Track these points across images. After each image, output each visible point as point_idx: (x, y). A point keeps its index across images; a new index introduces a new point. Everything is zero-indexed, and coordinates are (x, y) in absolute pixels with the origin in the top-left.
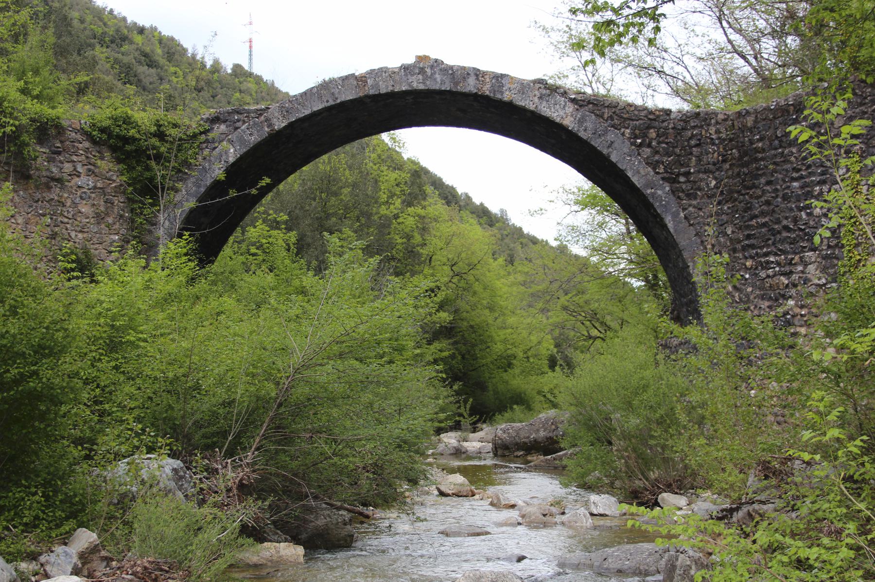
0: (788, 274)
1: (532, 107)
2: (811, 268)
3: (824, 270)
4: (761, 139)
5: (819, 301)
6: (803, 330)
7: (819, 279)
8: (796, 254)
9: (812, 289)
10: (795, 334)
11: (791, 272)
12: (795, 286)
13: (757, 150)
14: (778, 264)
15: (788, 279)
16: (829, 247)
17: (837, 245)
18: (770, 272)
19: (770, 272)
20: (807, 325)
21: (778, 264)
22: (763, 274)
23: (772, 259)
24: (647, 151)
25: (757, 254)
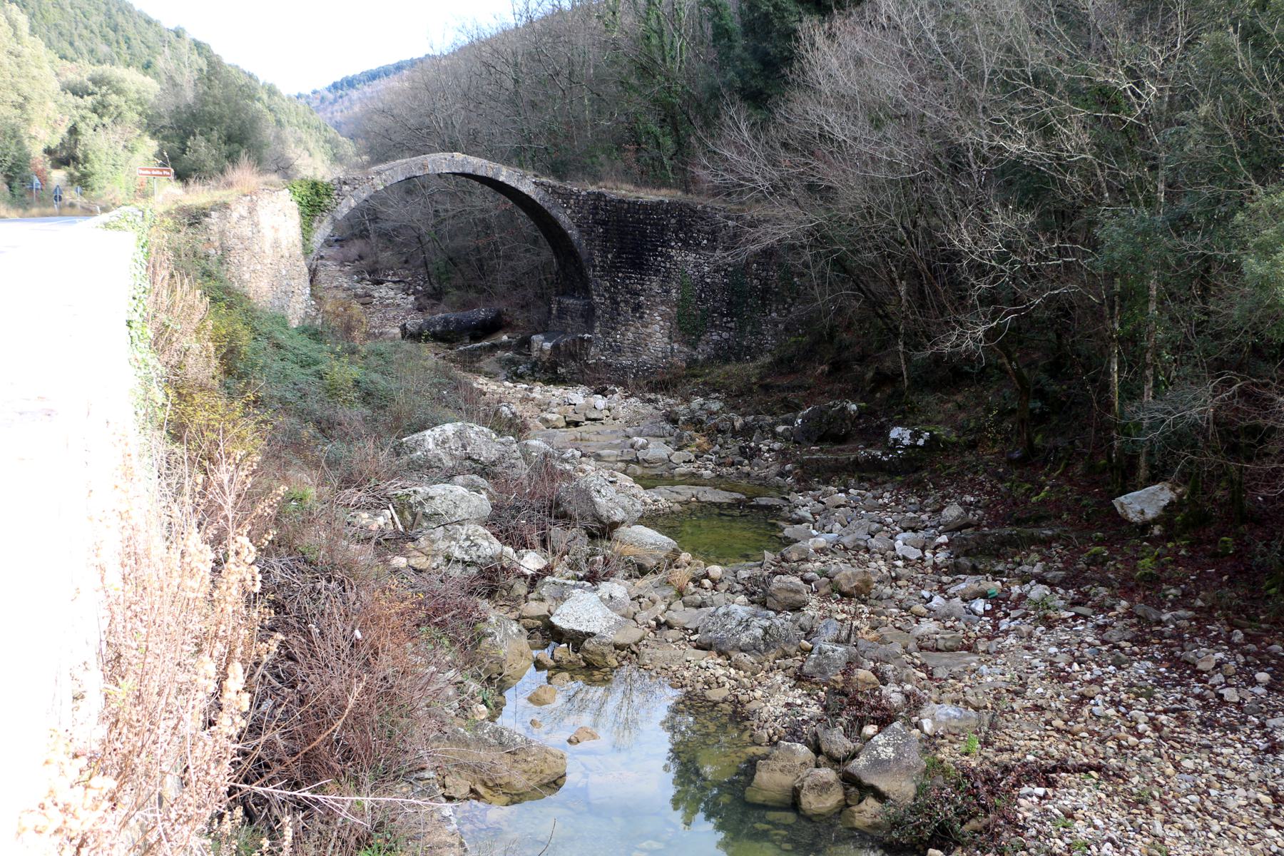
0: (642, 285)
1: (513, 185)
3: (661, 286)
5: (658, 300)
10: (643, 313)
20: (650, 309)
22: (628, 282)
24: (569, 211)
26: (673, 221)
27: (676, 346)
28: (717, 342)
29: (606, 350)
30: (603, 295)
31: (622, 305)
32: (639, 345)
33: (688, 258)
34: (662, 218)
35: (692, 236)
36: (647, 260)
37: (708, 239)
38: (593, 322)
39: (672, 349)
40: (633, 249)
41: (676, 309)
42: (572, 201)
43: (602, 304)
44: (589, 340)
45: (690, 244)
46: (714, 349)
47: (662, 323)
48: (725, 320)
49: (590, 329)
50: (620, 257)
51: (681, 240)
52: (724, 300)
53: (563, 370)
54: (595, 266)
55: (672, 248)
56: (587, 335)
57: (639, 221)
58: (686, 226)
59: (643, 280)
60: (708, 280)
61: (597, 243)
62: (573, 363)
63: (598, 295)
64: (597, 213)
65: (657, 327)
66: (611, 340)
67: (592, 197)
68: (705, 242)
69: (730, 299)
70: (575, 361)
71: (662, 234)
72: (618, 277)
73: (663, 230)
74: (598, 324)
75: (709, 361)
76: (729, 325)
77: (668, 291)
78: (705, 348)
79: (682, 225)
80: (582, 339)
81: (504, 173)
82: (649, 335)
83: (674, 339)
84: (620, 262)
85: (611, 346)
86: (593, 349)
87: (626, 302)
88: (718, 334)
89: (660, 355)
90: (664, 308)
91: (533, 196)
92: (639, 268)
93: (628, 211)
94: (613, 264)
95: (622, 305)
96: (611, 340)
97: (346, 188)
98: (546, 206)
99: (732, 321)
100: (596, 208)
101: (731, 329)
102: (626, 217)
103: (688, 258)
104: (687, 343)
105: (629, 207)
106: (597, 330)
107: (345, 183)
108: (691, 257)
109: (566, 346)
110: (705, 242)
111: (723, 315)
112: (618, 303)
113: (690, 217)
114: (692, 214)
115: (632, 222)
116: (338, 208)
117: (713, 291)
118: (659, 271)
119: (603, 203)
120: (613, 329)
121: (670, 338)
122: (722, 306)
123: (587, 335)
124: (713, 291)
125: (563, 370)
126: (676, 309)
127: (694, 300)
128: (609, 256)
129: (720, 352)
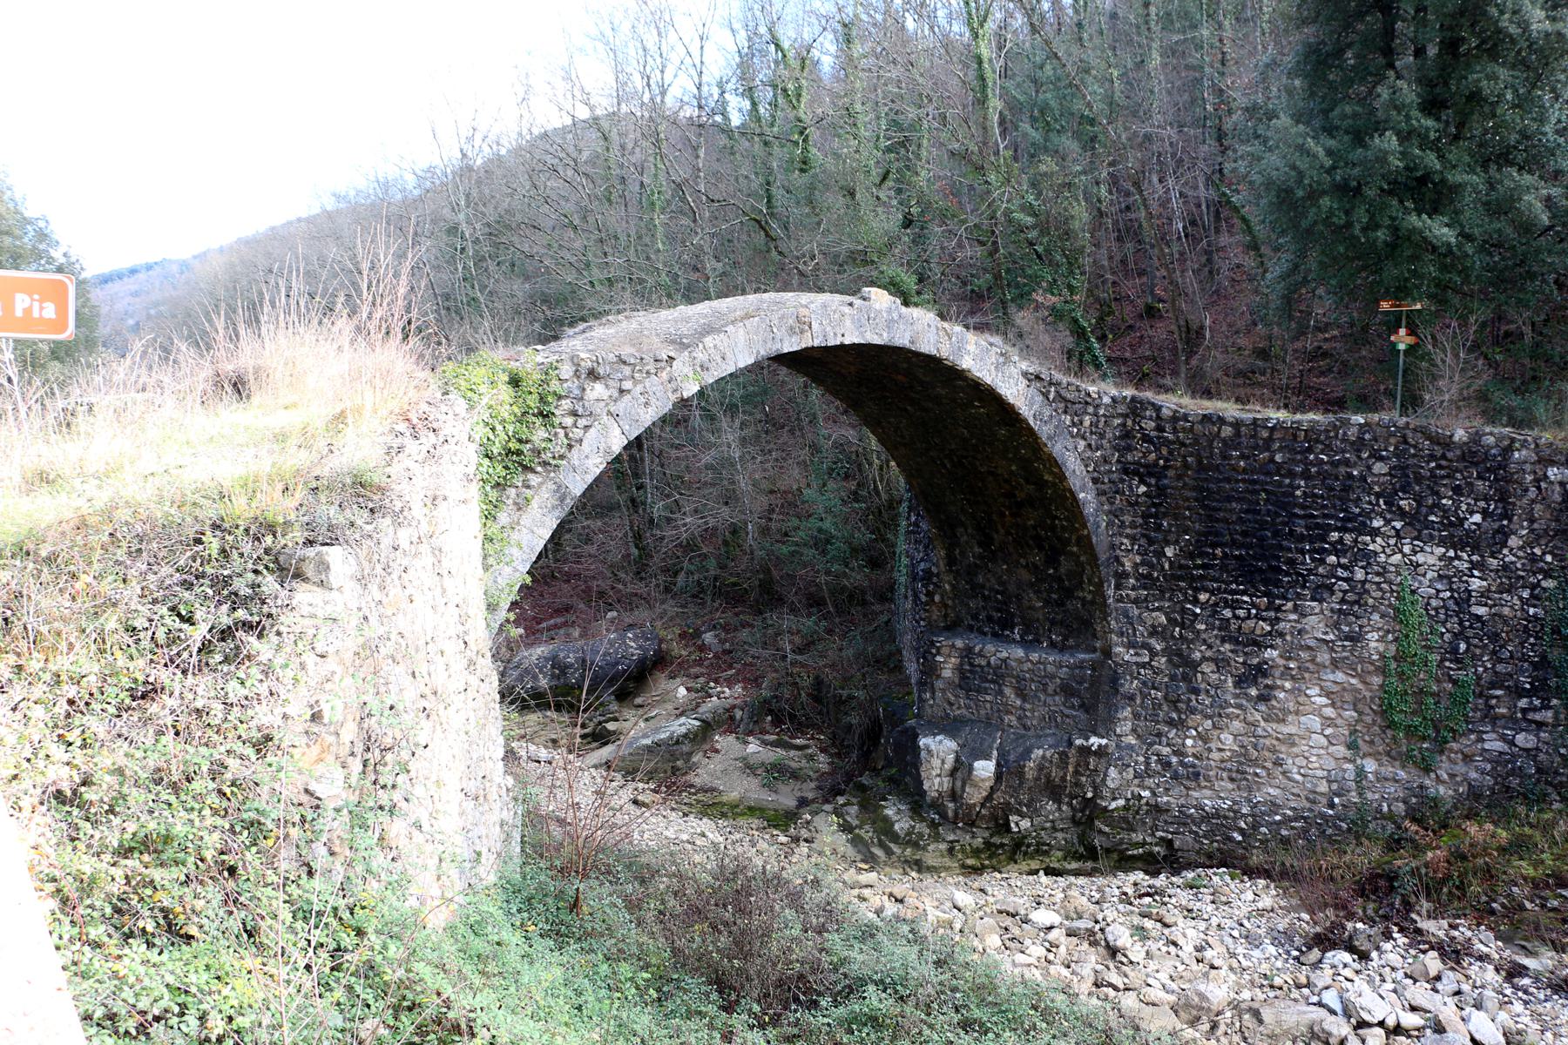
2: (1312, 620)
4: (1242, 456)
6: (1288, 685)
7: (1326, 633)
8: (1288, 600)
9: (1312, 643)
11: (1278, 620)
12: (1281, 635)
13: (1234, 469)
14: (1254, 605)
15: (1272, 625)
16: (1343, 601)
17: (1357, 602)
18: (1241, 613)
19: (1241, 613)
21: (1254, 605)
22: (1227, 613)
23: (1246, 598)
25: (1219, 589)
26: (1379, 468)
27: (1370, 766)
28: (1498, 760)
29: (1148, 773)
30: (1145, 646)
31: (1207, 668)
32: (1255, 763)
33: (1420, 558)
34: (1347, 463)
35: (1436, 505)
36: (1292, 562)
37: (1485, 513)
38: (1112, 709)
39: (1361, 773)
40: (1244, 534)
41: (1376, 680)
42: (1087, 420)
43: (1143, 665)
44: (1101, 752)
45: (1430, 525)
46: (1493, 773)
47: (1329, 712)
48: (1523, 703)
49: (1104, 725)
50: (1202, 555)
51: (1402, 514)
52: (1524, 658)
53: (1025, 824)
54: (1121, 576)
55: (1375, 533)
56: (1095, 741)
57: (1269, 468)
58: (1419, 479)
59: (1278, 609)
60: (1481, 611)
61: (1127, 519)
62: (1051, 806)
63: (1131, 645)
64: (1129, 448)
65: (1315, 722)
66: (1166, 750)
67: (1121, 409)
68: (1477, 518)
69: (1543, 657)
70: (1058, 801)
71: (1344, 500)
72: (1196, 602)
73: (1346, 489)
74: (1127, 712)
75: (1475, 803)
76: (1537, 717)
77: (1355, 638)
78: (1460, 768)
79: (1404, 477)
80: (1085, 751)
81: (971, 348)
82: (1290, 741)
83: (1364, 748)
84: (1204, 567)
85: (1167, 765)
86: (1113, 772)
87: (1221, 663)
88: (1503, 738)
89: (1323, 787)
90: (1340, 676)
91: (1025, 411)
92: (1266, 582)
93: (1229, 444)
94: (1180, 572)
95: (1207, 668)
96: (1166, 750)
97: (597, 390)
98: (1044, 431)
99: (1548, 707)
100: (1127, 435)
101: (1540, 725)
102: (1225, 457)
103: (1420, 558)
104: (1406, 759)
105: (1238, 434)
106: (1124, 727)
107: (593, 375)
108: (1431, 557)
109: (1041, 768)
110: (1477, 518)
111: (1520, 692)
112: (1194, 666)
113: (1432, 457)
114: (1439, 451)
115: (1244, 471)
116: (575, 455)
117: (1494, 637)
118: (1330, 589)
119: (1150, 425)
120: (1171, 723)
121: (1352, 746)
122: (1522, 671)
123: (1095, 741)
124: (1494, 637)
125: (1025, 824)
126: (1376, 680)
127: (1434, 658)
128: (1169, 552)
129: (1514, 782)
